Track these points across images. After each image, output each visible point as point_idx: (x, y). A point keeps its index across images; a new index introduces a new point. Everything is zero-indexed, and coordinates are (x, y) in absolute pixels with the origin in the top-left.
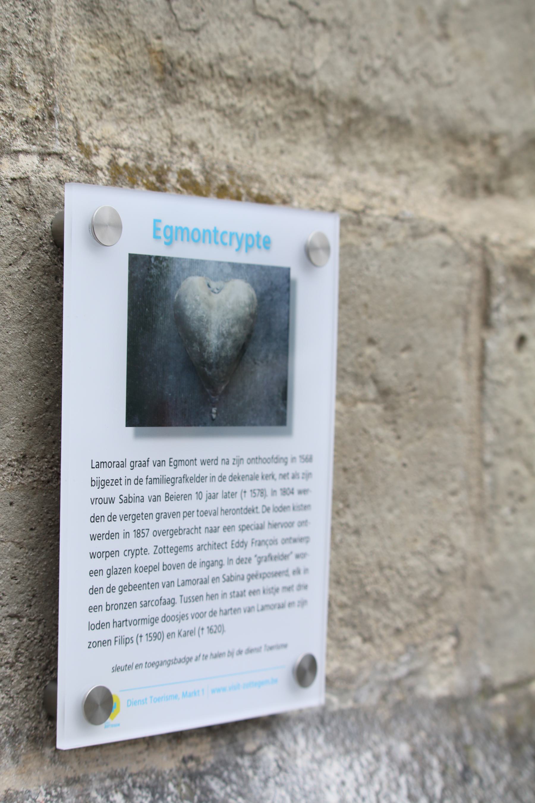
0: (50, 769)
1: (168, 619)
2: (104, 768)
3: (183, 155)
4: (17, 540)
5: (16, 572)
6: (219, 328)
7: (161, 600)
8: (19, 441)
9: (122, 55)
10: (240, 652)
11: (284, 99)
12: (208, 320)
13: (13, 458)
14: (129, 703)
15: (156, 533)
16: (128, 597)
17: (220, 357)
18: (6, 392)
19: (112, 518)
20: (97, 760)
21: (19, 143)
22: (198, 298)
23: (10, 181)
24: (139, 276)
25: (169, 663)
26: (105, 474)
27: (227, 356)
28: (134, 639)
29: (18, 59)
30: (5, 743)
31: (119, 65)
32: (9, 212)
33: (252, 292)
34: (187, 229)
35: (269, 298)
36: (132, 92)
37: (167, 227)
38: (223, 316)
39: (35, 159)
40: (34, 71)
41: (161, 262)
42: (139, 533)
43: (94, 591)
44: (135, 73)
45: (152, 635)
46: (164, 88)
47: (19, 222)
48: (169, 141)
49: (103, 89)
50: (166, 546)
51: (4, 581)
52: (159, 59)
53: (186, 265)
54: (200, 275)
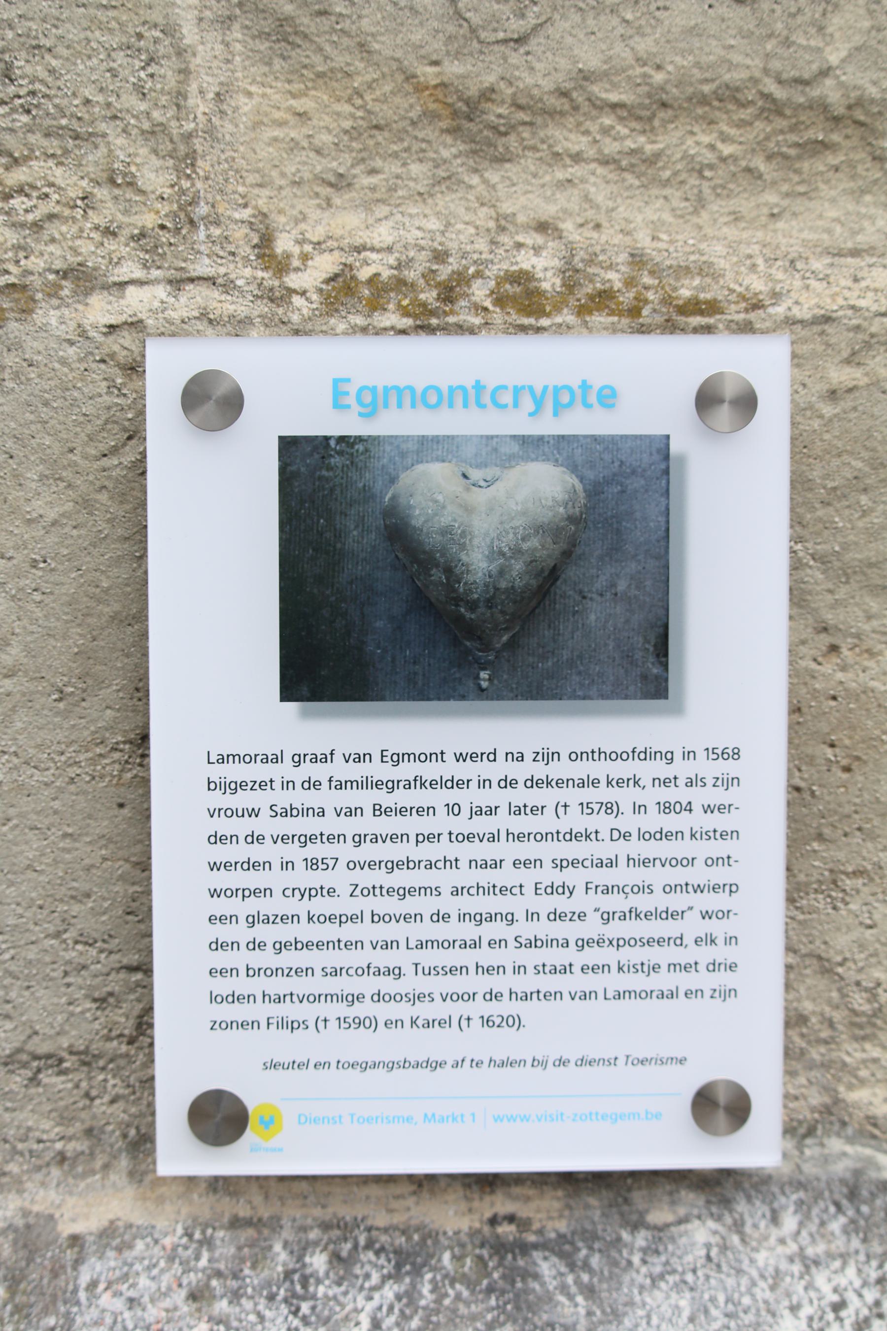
0: (204, 1199)
1: (387, 998)
2: (317, 1212)
3: (519, 246)
4: (133, 859)
5: (134, 905)
6: (492, 543)
7: (368, 967)
8: (130, 714)
9: (359, 102)
10: (562, 1062)
11: (759, 125)
12: (463, 532)
13: (120, 738)
14: (303, 1119)
15: (352, 865)
16: (290, 959)
17: (497, 589)
18: (102, 643)
19: (255, 839)
20: (306, 1197)
21: (125, 270)
22: (440, 498)
23: (105, 330)
24: (303, 469)
25: (391, 1066)
26: (235, 772)
27: (513, 587)
28: (311, 1024)
29: (120, 141)
30: (120, 1150)
31: (353, 116)
32: (101, 377)
33: (572, 480)
34: (411, 389)
35: (617, 489)
36: (395, 155)
37: (361, 390)
38: (501, 523)
39: (161, 292)
40: (157, 155)
41: (352, 445)
42: (313, 864)
43: (218, 945)
44: (394, 125)
45: (350, 1020)
46: (464, 142)
47: (119, 390)
48: (492, 224)
49: (323, 161)
50: (377, 885)
51: (111, 917)
52: (441, 97)
53: (411, 446)
54: (443, 461)
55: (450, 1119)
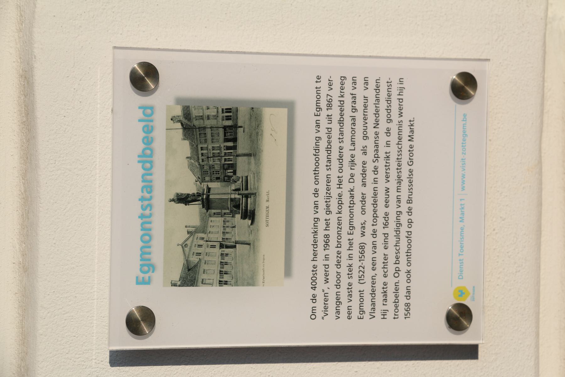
34: (142, 248)
55: (463, 210)
